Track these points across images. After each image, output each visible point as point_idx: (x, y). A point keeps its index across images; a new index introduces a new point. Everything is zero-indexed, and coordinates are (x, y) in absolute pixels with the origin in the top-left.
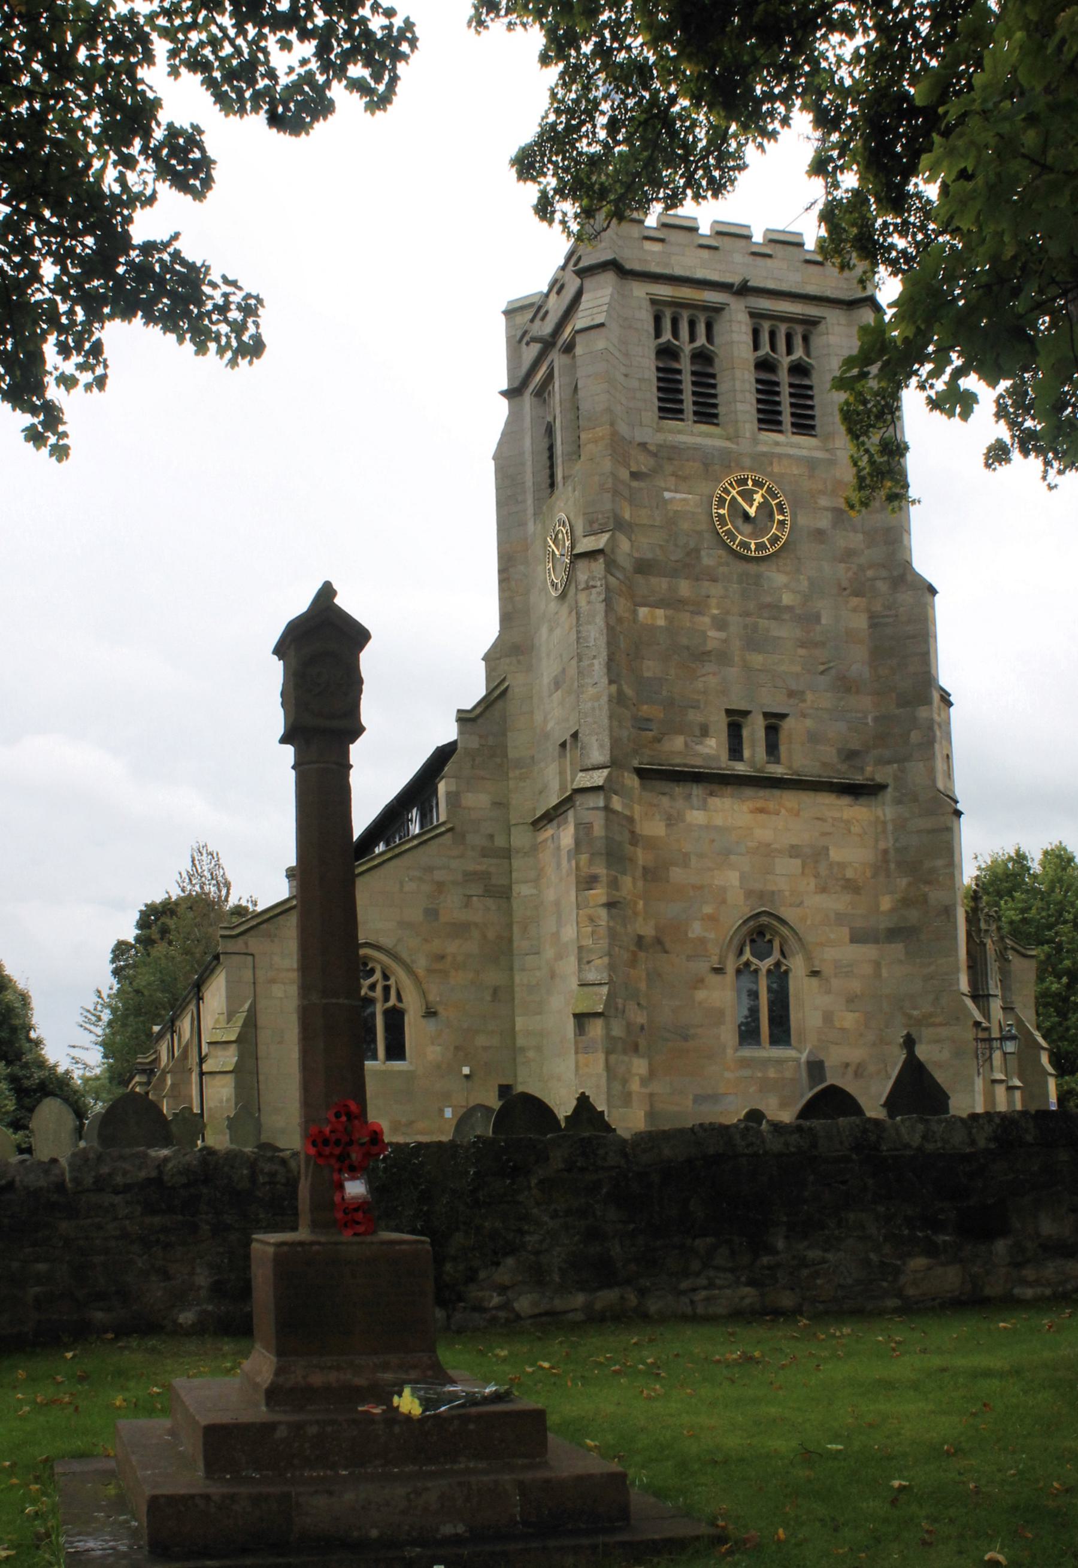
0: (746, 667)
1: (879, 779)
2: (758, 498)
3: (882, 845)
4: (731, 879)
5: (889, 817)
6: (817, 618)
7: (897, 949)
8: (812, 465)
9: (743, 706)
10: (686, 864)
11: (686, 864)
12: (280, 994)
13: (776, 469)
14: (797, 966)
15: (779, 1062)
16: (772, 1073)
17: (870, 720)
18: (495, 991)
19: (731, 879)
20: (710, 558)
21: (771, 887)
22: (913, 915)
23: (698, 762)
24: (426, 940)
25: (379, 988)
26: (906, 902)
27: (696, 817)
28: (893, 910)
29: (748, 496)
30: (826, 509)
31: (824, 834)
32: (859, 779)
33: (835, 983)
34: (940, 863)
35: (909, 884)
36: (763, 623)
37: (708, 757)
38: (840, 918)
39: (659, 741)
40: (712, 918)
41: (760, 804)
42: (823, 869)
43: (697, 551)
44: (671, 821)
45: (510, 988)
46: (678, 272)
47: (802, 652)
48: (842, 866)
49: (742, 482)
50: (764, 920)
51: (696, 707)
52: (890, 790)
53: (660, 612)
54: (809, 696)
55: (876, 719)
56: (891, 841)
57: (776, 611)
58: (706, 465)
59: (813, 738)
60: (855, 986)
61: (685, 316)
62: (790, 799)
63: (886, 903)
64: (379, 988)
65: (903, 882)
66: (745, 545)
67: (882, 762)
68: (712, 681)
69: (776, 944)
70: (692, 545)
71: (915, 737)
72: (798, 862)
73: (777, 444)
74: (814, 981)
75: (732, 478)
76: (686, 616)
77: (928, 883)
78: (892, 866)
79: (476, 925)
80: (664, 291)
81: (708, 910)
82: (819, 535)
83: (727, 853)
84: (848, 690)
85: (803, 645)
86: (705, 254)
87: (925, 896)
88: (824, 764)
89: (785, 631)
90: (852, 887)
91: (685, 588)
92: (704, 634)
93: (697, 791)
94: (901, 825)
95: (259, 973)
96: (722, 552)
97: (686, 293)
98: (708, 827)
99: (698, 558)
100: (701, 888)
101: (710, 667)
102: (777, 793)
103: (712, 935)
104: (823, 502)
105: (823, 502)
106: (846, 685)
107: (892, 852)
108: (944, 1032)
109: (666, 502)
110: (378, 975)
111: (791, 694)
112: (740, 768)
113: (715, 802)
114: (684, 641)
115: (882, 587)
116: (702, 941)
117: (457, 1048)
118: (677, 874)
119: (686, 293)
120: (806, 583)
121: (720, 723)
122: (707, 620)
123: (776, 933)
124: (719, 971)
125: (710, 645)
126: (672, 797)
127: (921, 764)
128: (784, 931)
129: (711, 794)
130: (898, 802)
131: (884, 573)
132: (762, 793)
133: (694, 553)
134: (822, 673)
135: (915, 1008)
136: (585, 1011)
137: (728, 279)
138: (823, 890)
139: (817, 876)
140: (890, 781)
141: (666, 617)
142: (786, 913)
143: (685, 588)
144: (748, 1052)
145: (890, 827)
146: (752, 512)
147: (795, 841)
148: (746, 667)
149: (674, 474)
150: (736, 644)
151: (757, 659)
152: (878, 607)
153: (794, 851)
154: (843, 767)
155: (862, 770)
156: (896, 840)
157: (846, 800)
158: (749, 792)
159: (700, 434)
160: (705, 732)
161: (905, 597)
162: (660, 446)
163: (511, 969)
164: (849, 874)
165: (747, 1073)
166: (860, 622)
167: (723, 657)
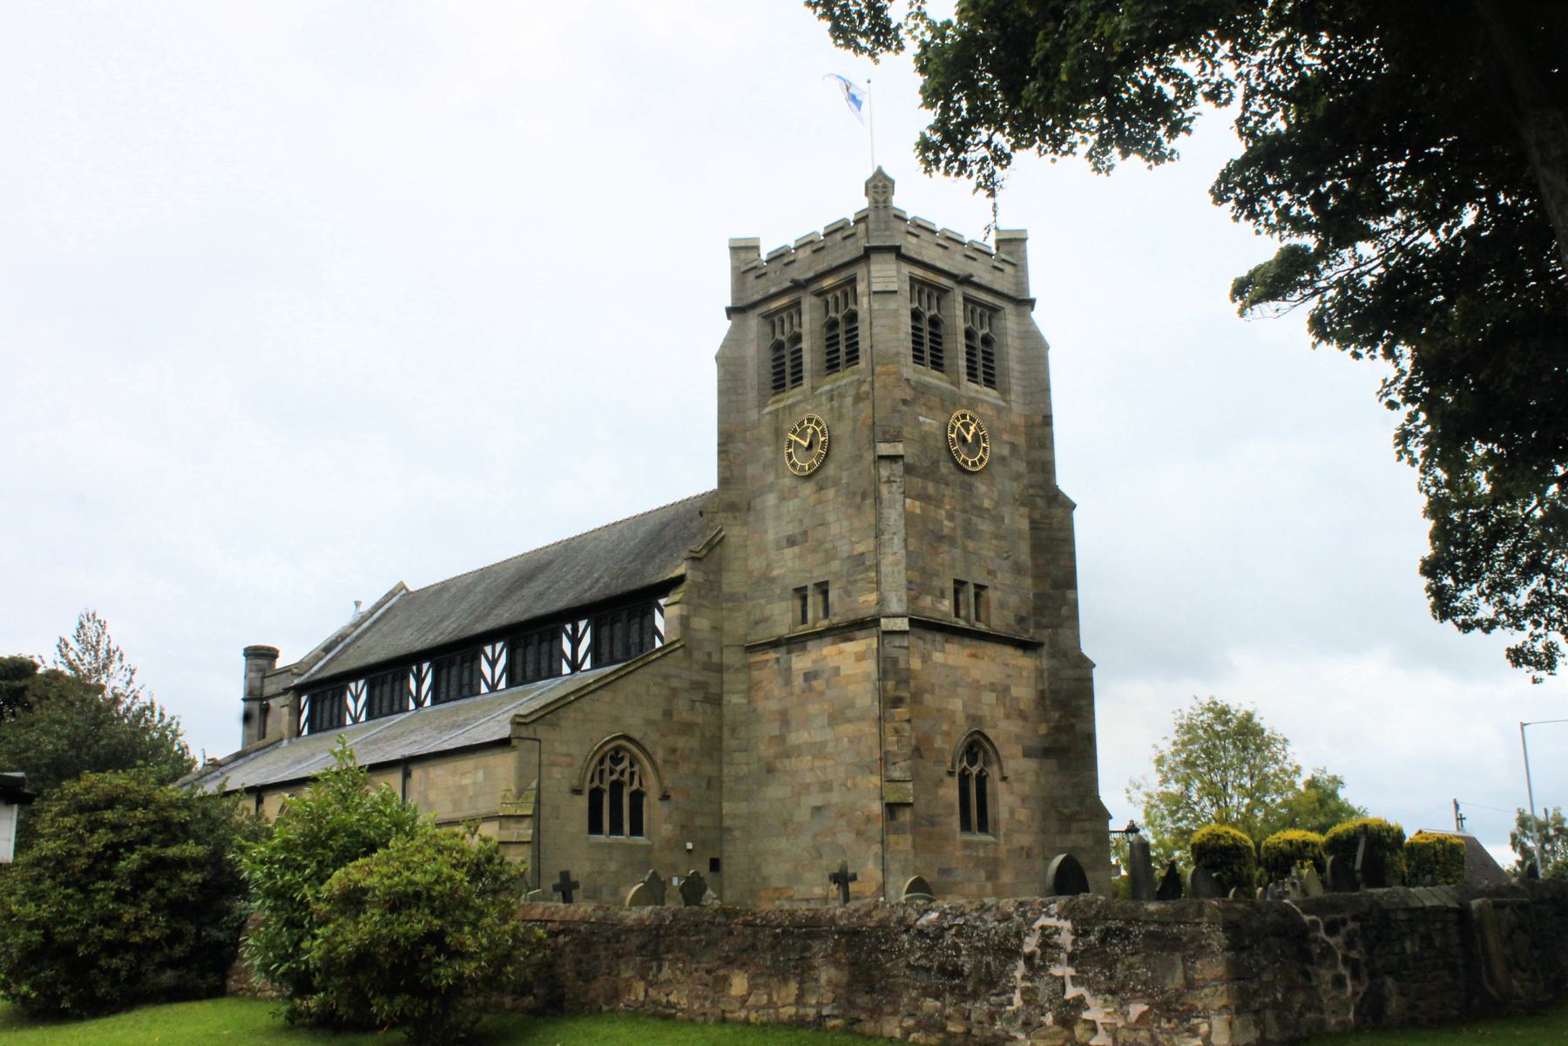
0: (965, 550)
1: (1038, 639)
2: (972, 429)
3: (1040, 687)
4: (957, 705)
5: (1045, 666)
6: (1002, 519)
7: (1052, 764)
8: (999, 409)
9: (961, 578)
10: (932, 693)
11: (932, 693)
12: (559, 776)
13: (980, 410)
14: (993, 772)
15: (986, 844)
16: (981, 854)
17: (1031, 595)
18: (709, 781)
19: (957, 705)
20: (945, 468)
21: (980, 713)
22: (1064, 739)
23: (938, 616)
24: (663, 735)
25: (627, 774)
26: (1058, 729)
27: (938, 657)
28: (1046, 735)
29: (966, 426)
30: (1007, 442)
31: (1009, 676)
32: (1025, 637)
33: (1016, 786)
34: (1083, 703)
35: (1061, 717)
36: (974, 519)
37: (945, 614)
38: (1018, 738)
39: (917, 598)
40: (947, 734)
41: (973, 651)
42: (1008, 704)
43: (938, 462)
44: (925, 658)
45: (720, 779)
46: (927, 259)
47: (994, 542)
48: (1017, 699)
49: (964, 416)
50: (977, 737)
51: (938, 576)
52: (1046, 647)
53: (917, 503)
54: (999, 575)
55: (1036, 595)
56: (1047, 684)
57: (980, 511)
58: (942, 400)
59: (1002, 605)
60: (1026, 789)
61: (926, 291)
62: (991, 649)
63: (1043, 729)
64: (627, 774)
65: (1056, 715)
66: (966, 462)
67: (1038, 626)
68: (946, 557)
69: (981, 755)
70: (935, 457)
71: (1064, 611)
72: (994, 695)
73: (986, 394)
74: (1004, 784)
75: (957, 413)
76: (932, 508)
77: (1074, 716)
78: (1048, 702)
79: (697, 724)
80: (919, 272)
81: (945, 727)
82: (1003, 459)
83: (956, 684)
84: (1019, 573)
85: (997, 537)
86: (940, 250)
87: (1073, 726)
88: (1008, 625)
89: (985, 526)
90: (1023, 716)
91: (931, 488)
92: (940, 522)
93: (939, 637)
94: (1054, 673)
95: (544, 757)
96: (951, 465)
97: (930, 276)
98: (944, 665)
99: (938, 467)
100: (939, 710)
101: (945, 547)
102: (983, 644)
103: (947, 747)
104: (1006, 437)
105: (1006, 437)
106: (1018, 569)
107: (1047, 694)
108: (1088, 825)
109: (921, 424)
110: (626, 763)
111: (990, 572)
112: (962, 623)
113: (949, 647)
114: (931, 527)
115: (1040, 502)
116: (941, 751)
117: (683, 827)
118: (928, 698)
119: (930, 276)
120: (996, 493)
121: (950, 586)
122: (943, 512)
123: (982, 747)
124: (951, 774)
125: (946, 531)
126: (924, 640)
127: (1069, 632)
128: (988, 746)
129: (947, 641)
130: (1052, 656)
131: (1041, 492)
132: (974, 642)
133: (935, 463)
134: (1006, 559)
135: (1066, 807)
136: (898, 801)
137: (954, 271)
138: (1007, 716)
139: (1004, 706)
140: (1046, 641)
141: (921, 508)
142: (990, 733)
143: (931, 488)
144: (967, 837)
145: (1046, 674)
146: (969, 438)
147: (993, 680)
148: (965, 550)
149: (925, 405)
150: (959, 532)
151: (971, 545)
152: (1037, 516)
153: (992, 687)
154: (1017, 628)
155: (1027, 631)
156: (1051, 684)
157: (1019, 652)
158: (967, 641)
159: (936, 377)
160: (943, 595)
161: (1058, 512)
162: (917, 382)
163: (720, 763)
164: (1022, 706)
165: (968, 852)
166: (1025, 525)
167: (952, 541)
